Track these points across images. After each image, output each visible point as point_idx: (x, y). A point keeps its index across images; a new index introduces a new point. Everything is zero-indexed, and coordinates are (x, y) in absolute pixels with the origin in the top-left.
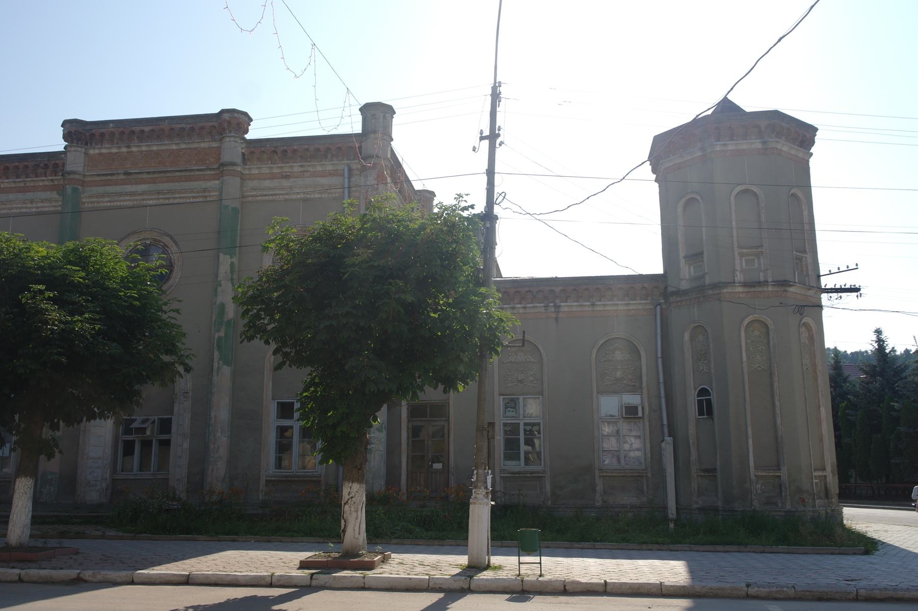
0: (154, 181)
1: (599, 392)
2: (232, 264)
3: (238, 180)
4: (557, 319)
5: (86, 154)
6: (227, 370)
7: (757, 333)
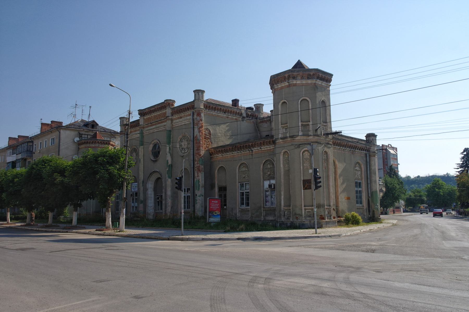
0: (155, 125)
1: (264, 180)
2: (169, 148)
3: (170, 121)
4: (252, 155)
5: (144, 119)
6: (170, 180)
7: (287, 156)
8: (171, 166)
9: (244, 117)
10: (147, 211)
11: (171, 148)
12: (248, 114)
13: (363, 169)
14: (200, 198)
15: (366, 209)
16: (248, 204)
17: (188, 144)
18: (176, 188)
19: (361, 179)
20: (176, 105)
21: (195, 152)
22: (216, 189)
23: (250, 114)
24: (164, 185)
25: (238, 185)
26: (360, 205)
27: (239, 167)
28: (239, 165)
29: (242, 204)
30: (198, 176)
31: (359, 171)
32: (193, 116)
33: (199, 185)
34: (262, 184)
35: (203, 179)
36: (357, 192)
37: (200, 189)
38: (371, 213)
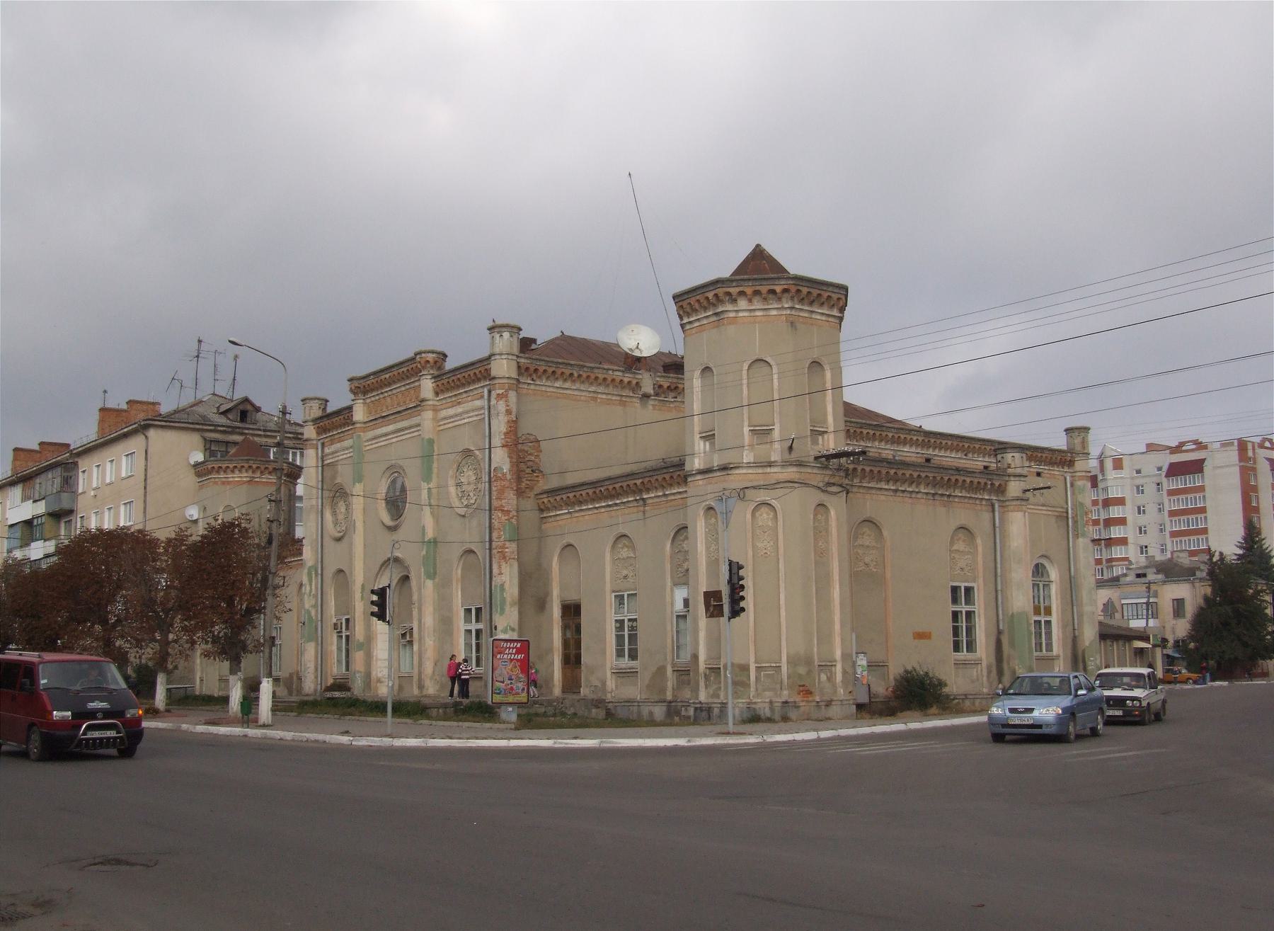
1: (676, 584)
6: (429, 583)
8: (435, 542)
9: (646, 396)
10: (374, 673)
11: (434, 491)
12: (660, 386)
16: (633, 656)
17: (478, 479)
18: (373, 614)
20: (450, 364)
21: (495, 503)
22: (556, 612)
23: (666, 385)
24: (415, 597)
25: (611, 598)
26: (970, 656)
27: (613, 547)
28: (612, 539)
29: (620, 653)
30: (501, 574)
32: (489, 400)
33: (503, 601)
34: (668, 599)
35: (516, 581)
36: (955, 615)
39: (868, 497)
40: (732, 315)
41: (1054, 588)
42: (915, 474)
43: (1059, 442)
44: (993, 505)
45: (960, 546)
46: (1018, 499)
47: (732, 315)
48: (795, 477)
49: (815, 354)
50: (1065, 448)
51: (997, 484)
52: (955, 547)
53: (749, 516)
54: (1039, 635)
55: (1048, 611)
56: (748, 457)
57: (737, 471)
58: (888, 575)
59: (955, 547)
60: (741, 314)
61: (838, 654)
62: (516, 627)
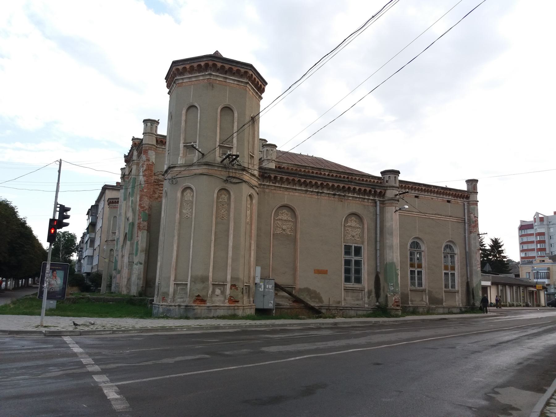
13: (366, 226)
14: (137, 266)
15: (370, 293)
19: (363, 243)
26: (357, 286)
31: (358, 228)
35: (145, 240)
36: (347, 262)
37: (139, 254)
38: (382, 299)
39: (286, 193)
40: (180, 81)
41: (456, 257)
42: (319, 183)
43: (463, 187)
44: (376, 203)
45: (353, 224)
46: (392, 199)
47: (180, 81)
48: (205, 171)
49: (227, 103)
50: (466, 189)
51: (378, 191)
52: (349, 224)
53: (179, 194)
54: (447, 280)
55: (453, 268)
56: (181, 161)
57: (176, 169)
58: (298, 236)
59: (349, 224)
60: (185, 81)
61: (229, 277)
62: (143, 262)
